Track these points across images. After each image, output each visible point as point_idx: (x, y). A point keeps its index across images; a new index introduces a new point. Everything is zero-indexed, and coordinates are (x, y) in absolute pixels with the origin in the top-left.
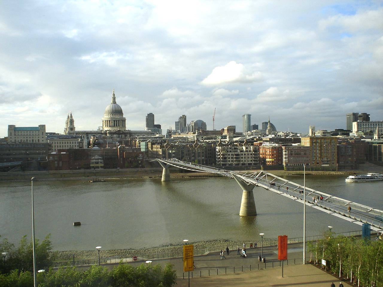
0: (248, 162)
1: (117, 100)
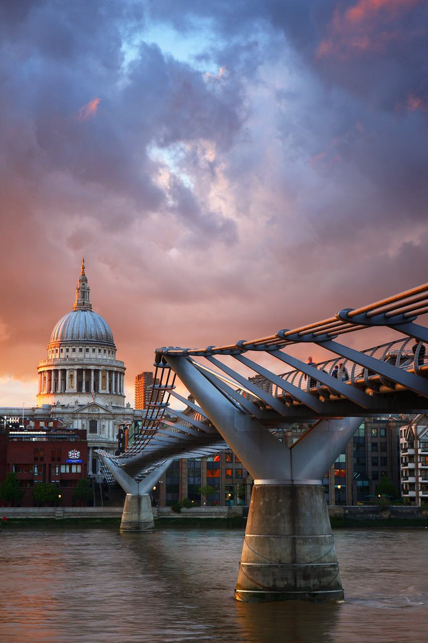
1: (92, 298)
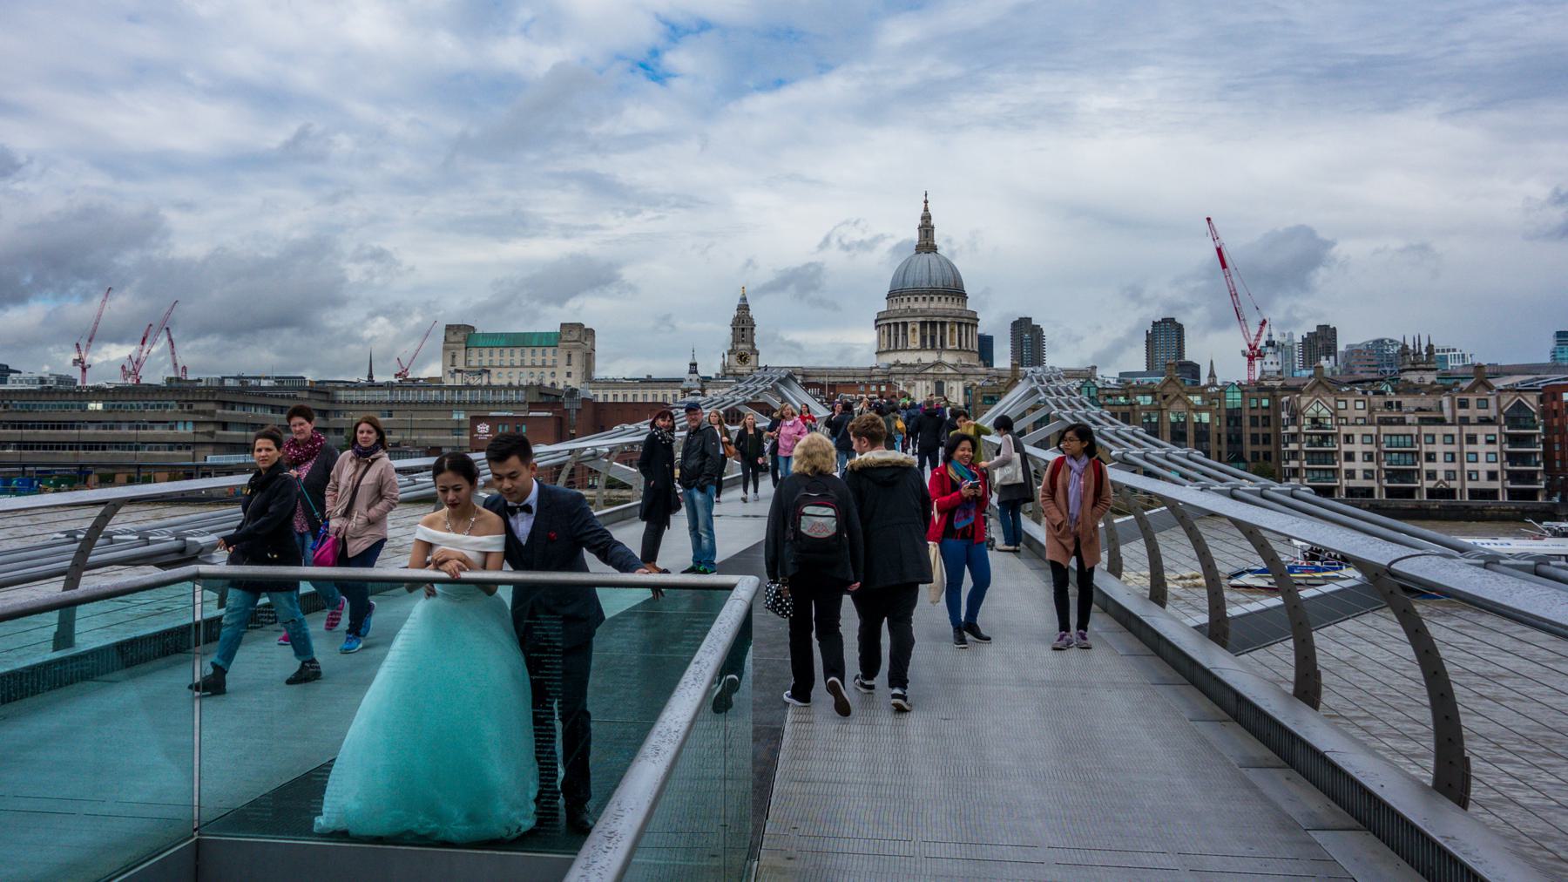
0: (1469, 485)
1: (938, 239)
